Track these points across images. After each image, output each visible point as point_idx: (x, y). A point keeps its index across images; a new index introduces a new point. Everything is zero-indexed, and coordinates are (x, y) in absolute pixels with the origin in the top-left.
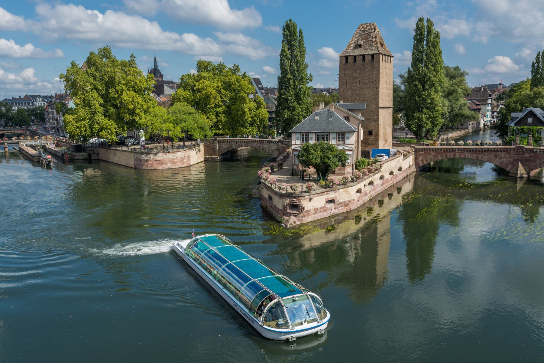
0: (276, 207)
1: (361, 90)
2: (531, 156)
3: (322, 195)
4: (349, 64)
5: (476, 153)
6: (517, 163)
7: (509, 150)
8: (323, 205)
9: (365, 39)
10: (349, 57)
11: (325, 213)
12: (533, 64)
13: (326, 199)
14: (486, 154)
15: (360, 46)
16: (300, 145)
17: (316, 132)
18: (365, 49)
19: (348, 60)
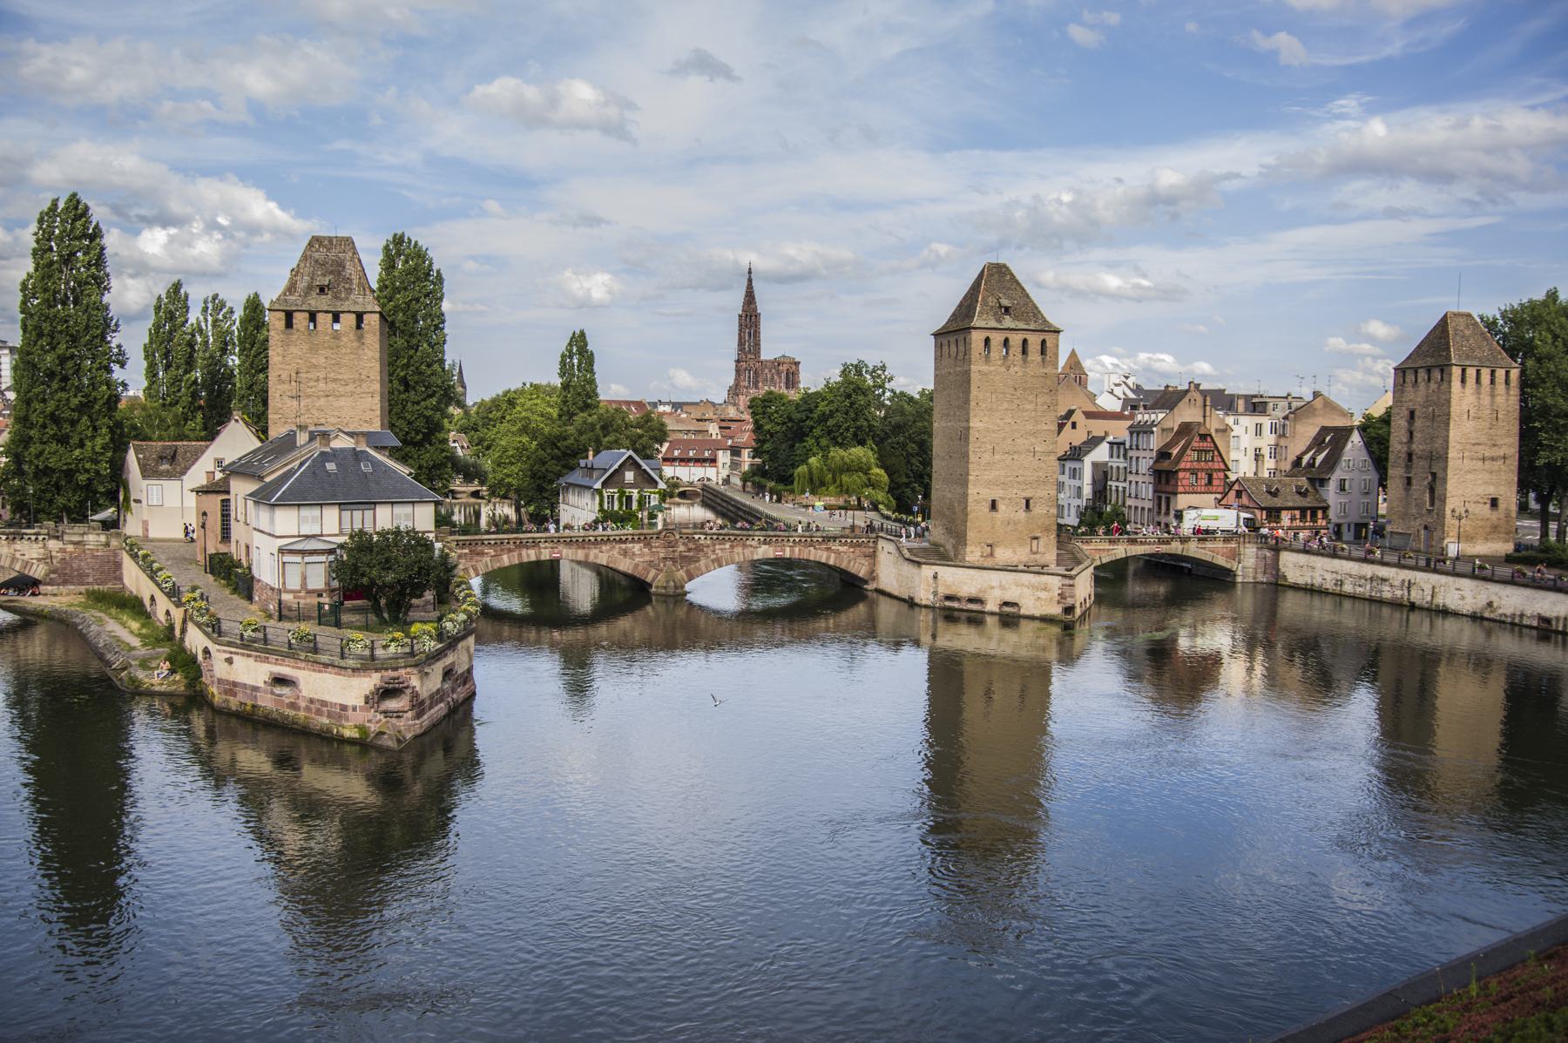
0: (324, 703)
1: (330, 398)
2: (689, 550)
3: (439, 659)
4: (298, 331)
5: (584, 548)
6: (665, 565)
7: (648, 537)
8: (439, 686)
9: (331, 273)
10: (295, 314)
11: (442, 705)
12: (563, 356)
13: (444, 669)
14: (604, 548)
15: (322, 290)
16: (299, 536)
17: (340, 504)
18: (336, 297)
19: (294, 321)
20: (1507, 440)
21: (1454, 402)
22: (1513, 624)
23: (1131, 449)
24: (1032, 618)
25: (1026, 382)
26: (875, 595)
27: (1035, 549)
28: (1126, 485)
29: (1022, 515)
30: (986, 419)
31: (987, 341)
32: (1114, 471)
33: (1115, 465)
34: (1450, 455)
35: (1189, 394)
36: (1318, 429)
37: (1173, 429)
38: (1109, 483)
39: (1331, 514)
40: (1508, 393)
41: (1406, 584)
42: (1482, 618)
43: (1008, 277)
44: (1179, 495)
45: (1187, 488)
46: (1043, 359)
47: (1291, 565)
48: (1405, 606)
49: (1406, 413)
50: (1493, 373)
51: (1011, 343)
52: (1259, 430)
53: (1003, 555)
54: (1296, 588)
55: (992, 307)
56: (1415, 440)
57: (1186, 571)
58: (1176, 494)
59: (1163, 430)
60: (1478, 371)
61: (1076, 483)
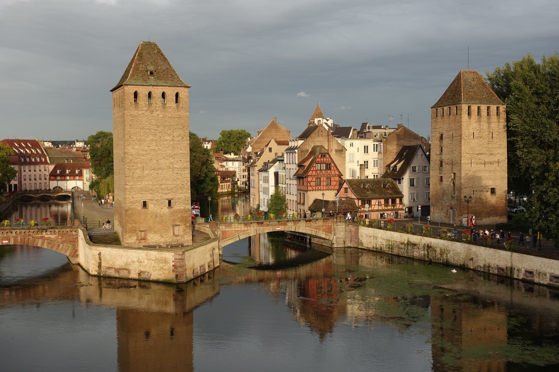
20: (499, 151)
21: (463, 128)
22: (484, 272)
23: (287, 163)
24: (157, 282)
25: (165, 121)
26: (79, 267)
27: (176, 233)
28: (284, 186)
29: (166, 210)
30: (137, 147)
31: (136, 94)
32: (281, 176)
33: (281, 174)
34: (462, 162)
35: (318, 128)
36: (401, 148)
37: (308, 150)
38: (280, 185)
39: (406, 200)
40: (499, 121)
41: (426, 248)
42: (470, 269)
43: (156, 52)
44: (309, 192)
45: (314, 188)
46: (177, 107)
47: (365, 236)
48: (427, 261)
49: (439, 135)
50: (488, 108)
51: (153, 95)
52: (366, 149)
53: (153, 238)
54: (368, 250)
55: (141, 71)
56: (444, 152)
57: (308, 241)
58: (307, 191)
59: (302, 151)
60: (479, 108)
61: (266, 185)
